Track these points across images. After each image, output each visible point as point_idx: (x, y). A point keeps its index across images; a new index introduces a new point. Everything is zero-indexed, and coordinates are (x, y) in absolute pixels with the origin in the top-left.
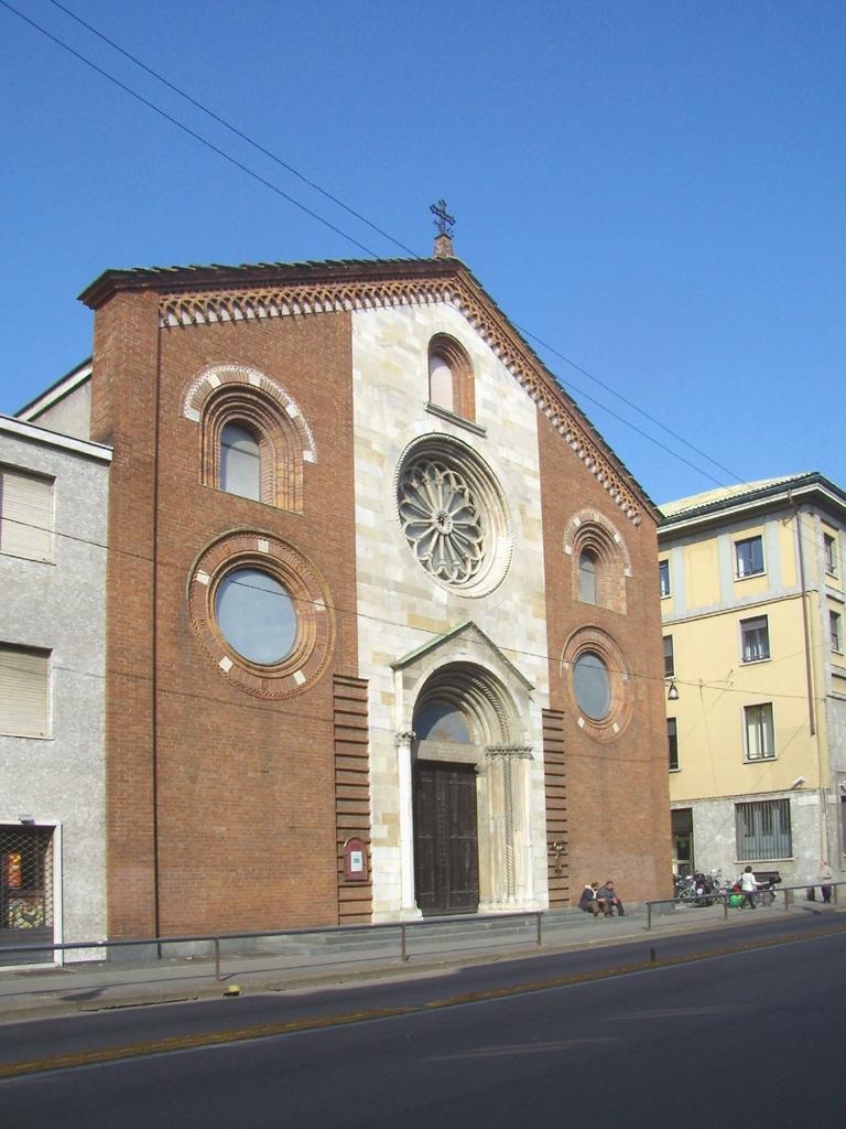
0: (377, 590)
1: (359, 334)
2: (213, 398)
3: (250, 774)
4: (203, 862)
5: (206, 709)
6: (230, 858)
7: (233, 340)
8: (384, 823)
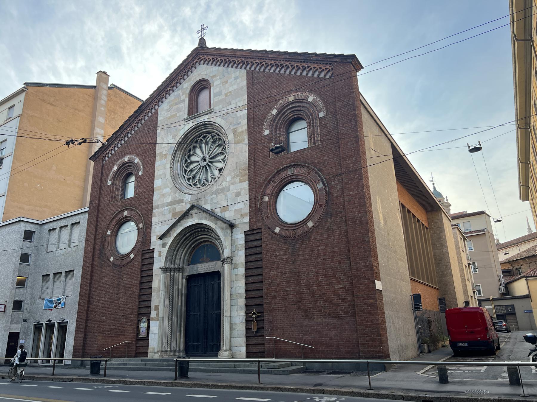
1: (161, 114)
2: (116, 174)
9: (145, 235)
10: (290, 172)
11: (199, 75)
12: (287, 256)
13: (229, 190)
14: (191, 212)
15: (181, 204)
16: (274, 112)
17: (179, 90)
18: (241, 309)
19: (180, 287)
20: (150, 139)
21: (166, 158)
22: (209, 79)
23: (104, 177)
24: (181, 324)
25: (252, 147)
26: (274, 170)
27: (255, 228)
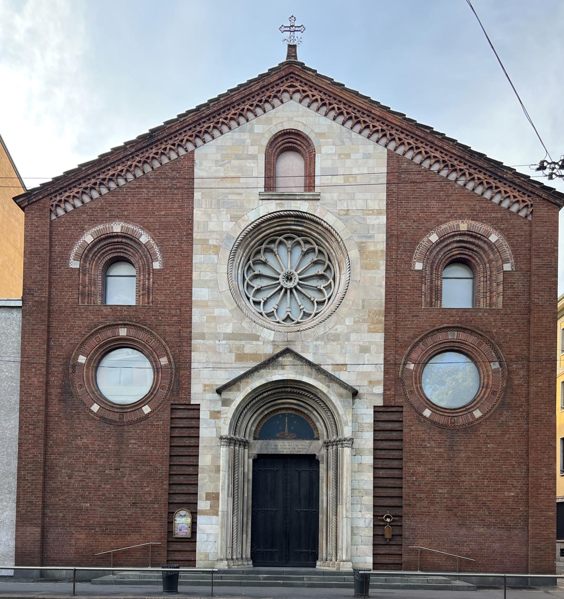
0: (210, 342)
1: (201, 164)
3: (107, 472)
4: (74, 524)
5: (80, 436)
6: (91, 522)
7: (102, 209)
8: (207, 499)
9: (174, 378)
10: (452, 336)
11: (290, 119)
12: (441, 450)
13: (348, 339)
14: (280, 359)
15: (254, 342)
16: (434, 238)
17: (244, 131)
18: (368, 510)
19: (246, 470)
20: (176, 205)
21: (217, 253)
22: (312, 136)
23: (57, 249)
24: (247, 523)
25: (394, 282)
26: (428, 328)
27: (393, 404)
